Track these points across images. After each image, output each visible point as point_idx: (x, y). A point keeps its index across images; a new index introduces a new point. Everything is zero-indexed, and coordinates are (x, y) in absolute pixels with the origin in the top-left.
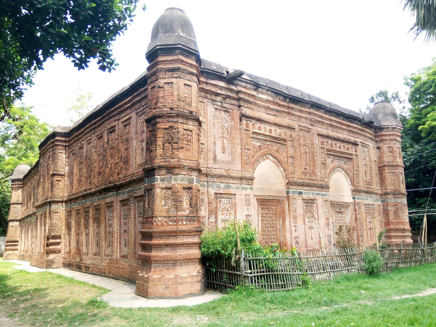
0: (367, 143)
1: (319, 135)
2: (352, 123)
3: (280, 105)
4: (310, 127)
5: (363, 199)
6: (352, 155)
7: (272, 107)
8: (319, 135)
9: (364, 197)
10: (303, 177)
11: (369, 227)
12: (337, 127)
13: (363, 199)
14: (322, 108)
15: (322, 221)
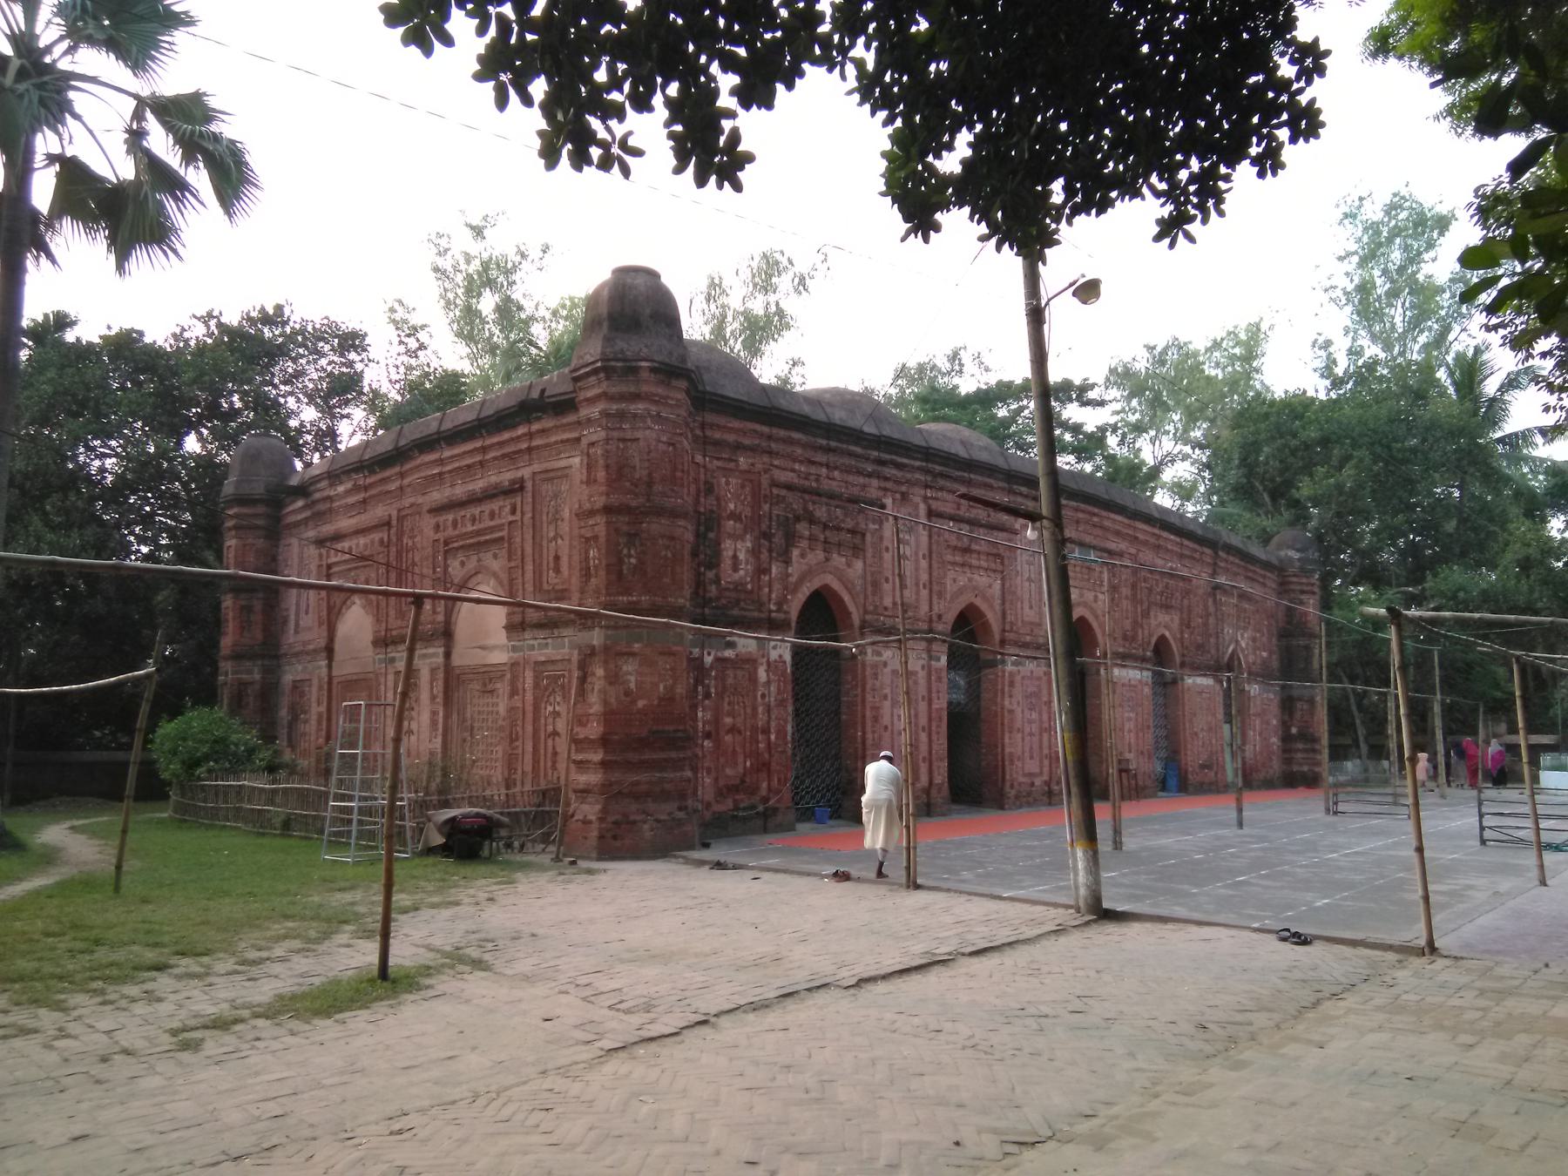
0: (562, 464)
1: (430, 511)
2: (514, 426)
3: (366, 488)
4: (420, 500)
5: (532, 648)
6: (499, 528)
7: (351, 500)
8: (430, 511)
9: (535, 643)
10: (399, 622)
11: (550, 728)
12: (469, 466)
13: (532, 648)
14: (438, 441)
15: (425, 717)
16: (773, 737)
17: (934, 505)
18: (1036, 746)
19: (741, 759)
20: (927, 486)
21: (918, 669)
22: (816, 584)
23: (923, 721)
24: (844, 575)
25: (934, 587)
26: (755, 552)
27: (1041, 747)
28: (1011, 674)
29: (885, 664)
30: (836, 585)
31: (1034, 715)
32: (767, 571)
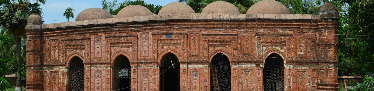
16: (61, 84)
17: (107, 35)
18: (147, 86)
19: (56, 87)
20: (104, 32)
21: (103, 70)
22: (73, 56)
23: (104, 81)
24: (82, 54)
25: (108, 52)
26: (58, 53)
27: (149, 87)
28: (134, 70)
29: (92, 70)
30: (78, 56)
31: (146, 79)
32: (60, 56)
